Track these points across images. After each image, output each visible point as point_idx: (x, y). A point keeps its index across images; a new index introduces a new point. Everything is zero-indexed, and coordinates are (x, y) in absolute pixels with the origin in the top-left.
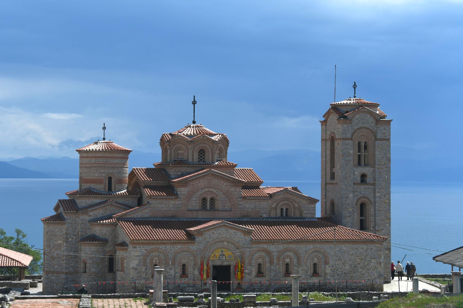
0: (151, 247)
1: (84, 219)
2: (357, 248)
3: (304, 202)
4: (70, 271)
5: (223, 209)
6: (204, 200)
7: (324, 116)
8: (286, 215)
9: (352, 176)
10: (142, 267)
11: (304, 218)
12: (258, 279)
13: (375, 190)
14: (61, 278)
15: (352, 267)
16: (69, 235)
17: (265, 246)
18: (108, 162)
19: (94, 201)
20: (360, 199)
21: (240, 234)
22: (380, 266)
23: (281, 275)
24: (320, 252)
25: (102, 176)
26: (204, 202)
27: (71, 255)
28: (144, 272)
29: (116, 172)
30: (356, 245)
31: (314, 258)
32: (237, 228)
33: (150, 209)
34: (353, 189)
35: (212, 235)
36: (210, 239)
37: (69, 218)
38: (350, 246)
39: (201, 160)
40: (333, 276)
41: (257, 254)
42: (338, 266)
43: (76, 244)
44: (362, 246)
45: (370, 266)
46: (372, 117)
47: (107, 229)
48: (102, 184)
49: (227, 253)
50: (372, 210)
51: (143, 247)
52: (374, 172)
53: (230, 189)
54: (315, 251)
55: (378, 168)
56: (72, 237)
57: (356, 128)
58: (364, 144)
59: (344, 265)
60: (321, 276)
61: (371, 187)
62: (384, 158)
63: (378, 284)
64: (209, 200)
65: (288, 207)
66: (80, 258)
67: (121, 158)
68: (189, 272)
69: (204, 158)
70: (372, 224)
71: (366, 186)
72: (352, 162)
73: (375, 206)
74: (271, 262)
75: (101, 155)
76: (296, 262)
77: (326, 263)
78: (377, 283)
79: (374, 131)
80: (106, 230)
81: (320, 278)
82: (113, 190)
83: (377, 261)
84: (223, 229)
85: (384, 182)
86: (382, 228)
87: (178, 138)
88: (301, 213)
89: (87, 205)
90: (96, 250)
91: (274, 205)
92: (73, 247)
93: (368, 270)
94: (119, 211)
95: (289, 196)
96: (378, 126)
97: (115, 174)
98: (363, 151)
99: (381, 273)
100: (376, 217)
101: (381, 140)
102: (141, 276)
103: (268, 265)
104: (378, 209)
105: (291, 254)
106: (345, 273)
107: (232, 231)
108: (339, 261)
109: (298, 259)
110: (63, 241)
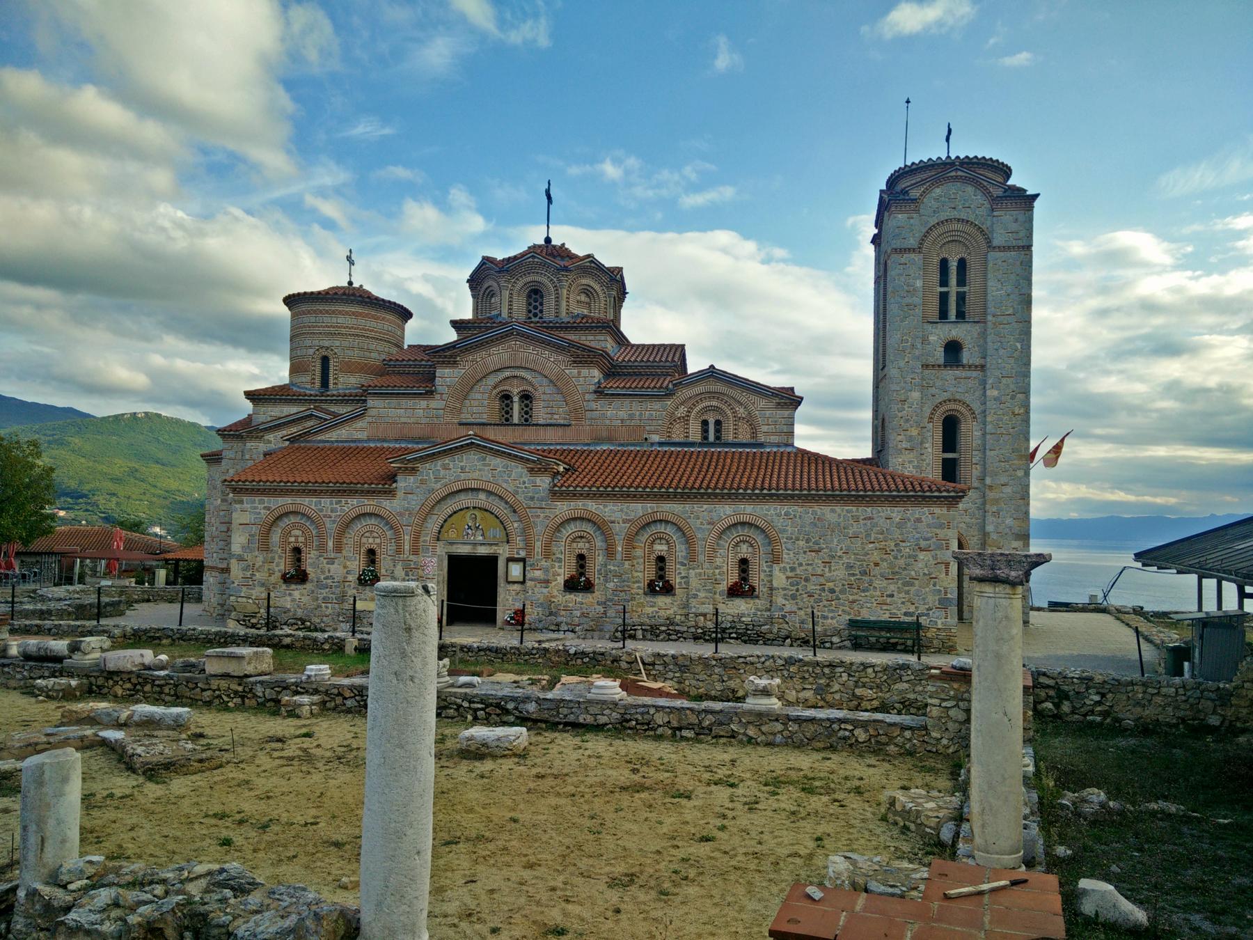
0: (281, 501)
2: (870, 518)
3: (762, 403)
5: (549, 421)
6: (506, 397)
7: (876, 226)
8: (718, 438)
9: (919, 346)
10: (257, 553)
11: (761, 445)
12: (572, 596)
13: (983, 383)
15: (854, 575)
17: (592, 506)
20: (940, 403)
21: (520, 470)
22: (947, 574)
23: (639, 588)
24: (757, 527)
26: (507, 405)
28: (260, 566)
29: (338, 343)
30: (869, 510)
31: (741, 544)
32: (510, 454)
33: (370, 419)
34: (923, 379)
35: (442, 472)
36: (436, 482)
38: (848, 511)
39: (535, 315)
40: (794, 597)
42: (810, 568)
45: (913, 573)
46: (978, 192)
50: (975, 433)
51: (261, 502)
52: (983, 335)
53: (567, 371)
54: (743, 524)
55: (994, 324)
57: (933, 221)
58: (956, 264)
59: (830, 567)
60: (757, 597)
61: (974, 374)
62: (1012, 296)
63: (940, 627)
64: (516, 399)
65: (720, 418)
67: (353, 313)
68: (383, 571)
69: (541, 311)
70: (976, 472)
71: (958, 373)
72: (918, 311)
73: (984, 423)
74: (610, 552)
76: (684, 554)
77: (775, 559)
78: (936, 623)
79: (984, 227)
81: (757, 601)
82: (331, 386)
83: (935, 557)
84: (472, 456)
85: (1012, 361)
86: (1003, 479)
88: (754, 434)
89: (269, 419)
91: (682, 411)
93: (906, 584)
95: (720, 387)
96: (995, 213)
98: (953, 280)
99: (949, 596)
100: (988, 453)
102: (254, 578)
103: (600, 558)
104: (993, 431)
105: (670, 530)
106: (832, 591)
107: (497, 462)
108: (813, 554)
109: (689, 541)
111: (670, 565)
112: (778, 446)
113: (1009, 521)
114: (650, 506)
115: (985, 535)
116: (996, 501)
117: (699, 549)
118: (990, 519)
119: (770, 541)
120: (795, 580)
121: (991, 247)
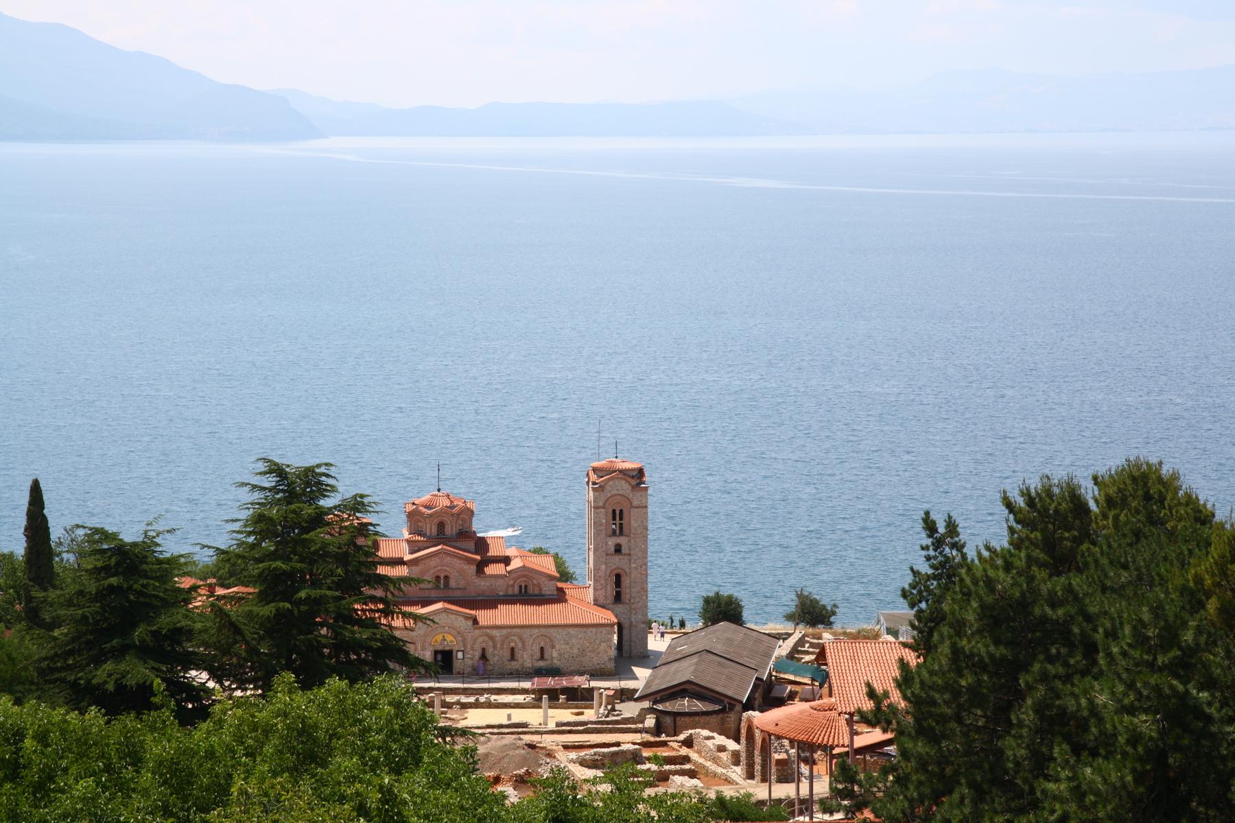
3: (544, 579)
6: (438, 578)
8: (526, 591)
11: (543, 595)
13: (630, 560)
17: (488, 631)
41: (481, 639)
44: (591, 629)
49: (449, 638)
52: (629, 541)
57: (609, 495)
71: (621, 557)
72: (604, 532)
74: (495, 647)
77: (553, 647)
86: (637, 600)
88: (540, 590)
91: (511, 582)
101: (637, 507)
105: (516, 638)
109: (523, 642)
111: (516, 650)
112: (550, 595)
113: (640, 617)
114: (509, 630)
115: (631, 622)
116: (635, 609)
117: (526, 644)
118: (633, 616)
119: (551, 641)
120: (560, 655)
121: (632, 507)
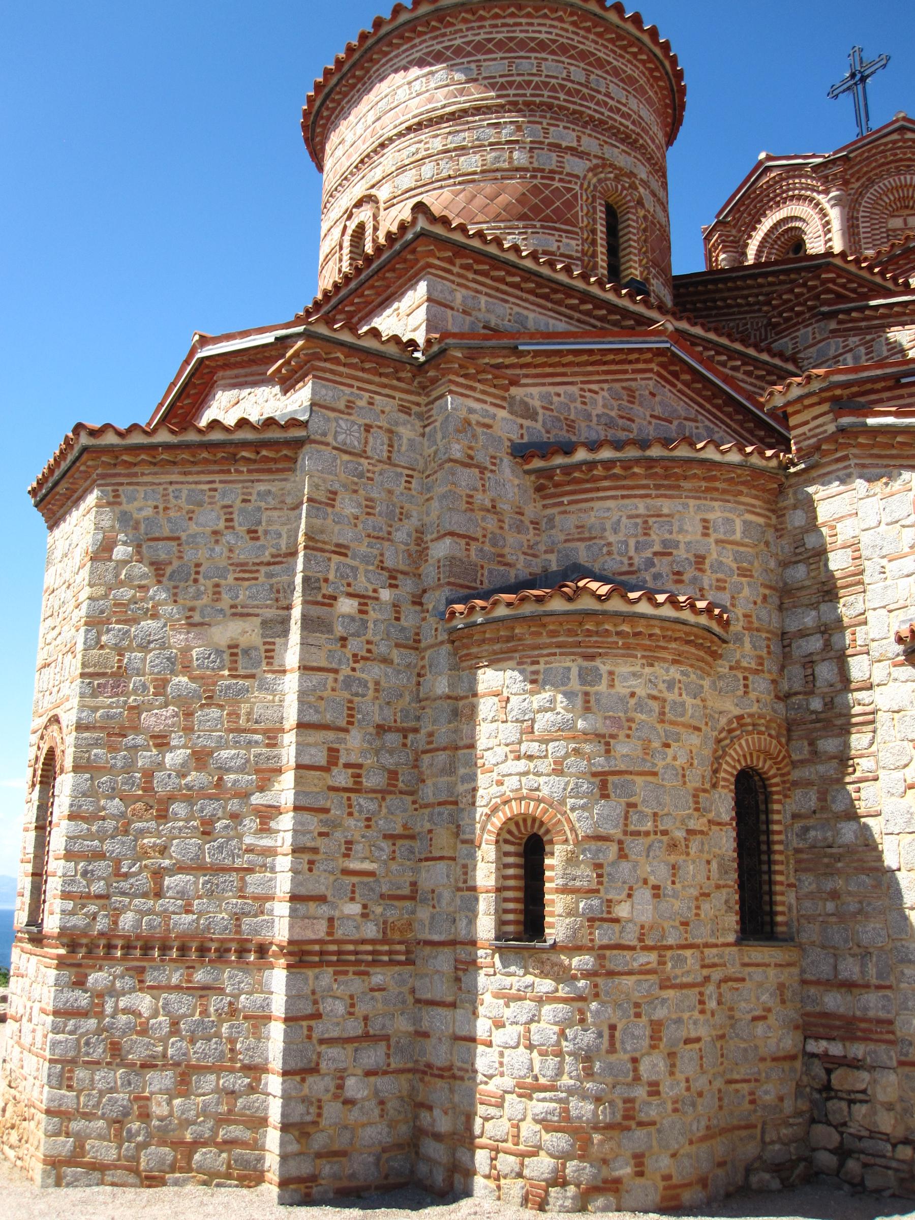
1: (478, 423)
4: (339, 934)
14: (233, 1011)
16: (336, 558)
18: (599, 92)
19: (531, 315)
25: (568, 169)
27: (347, 766)
37: (341, 405)
43: (395, 654)
47: (710, 516)
48: (567, 222)
56: (362, 584)
66: (451, 788)
75: (553, 37)
80: (705, 521)
87: (895, 137)
90: (654, 698)
92: (371, 685)
94: (707, 428)
97: (641, 190)
110: (264, 623)
